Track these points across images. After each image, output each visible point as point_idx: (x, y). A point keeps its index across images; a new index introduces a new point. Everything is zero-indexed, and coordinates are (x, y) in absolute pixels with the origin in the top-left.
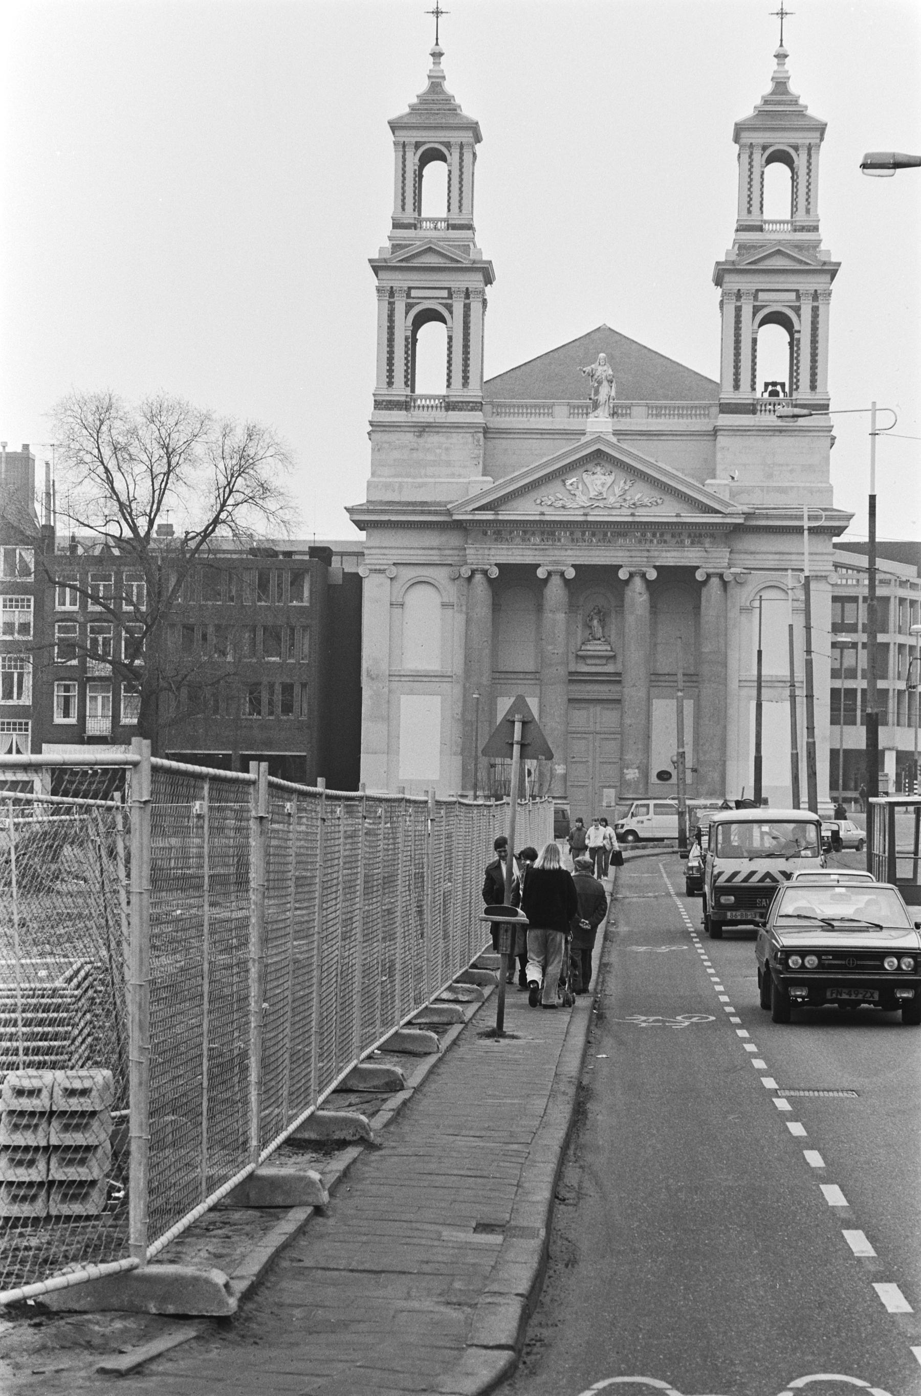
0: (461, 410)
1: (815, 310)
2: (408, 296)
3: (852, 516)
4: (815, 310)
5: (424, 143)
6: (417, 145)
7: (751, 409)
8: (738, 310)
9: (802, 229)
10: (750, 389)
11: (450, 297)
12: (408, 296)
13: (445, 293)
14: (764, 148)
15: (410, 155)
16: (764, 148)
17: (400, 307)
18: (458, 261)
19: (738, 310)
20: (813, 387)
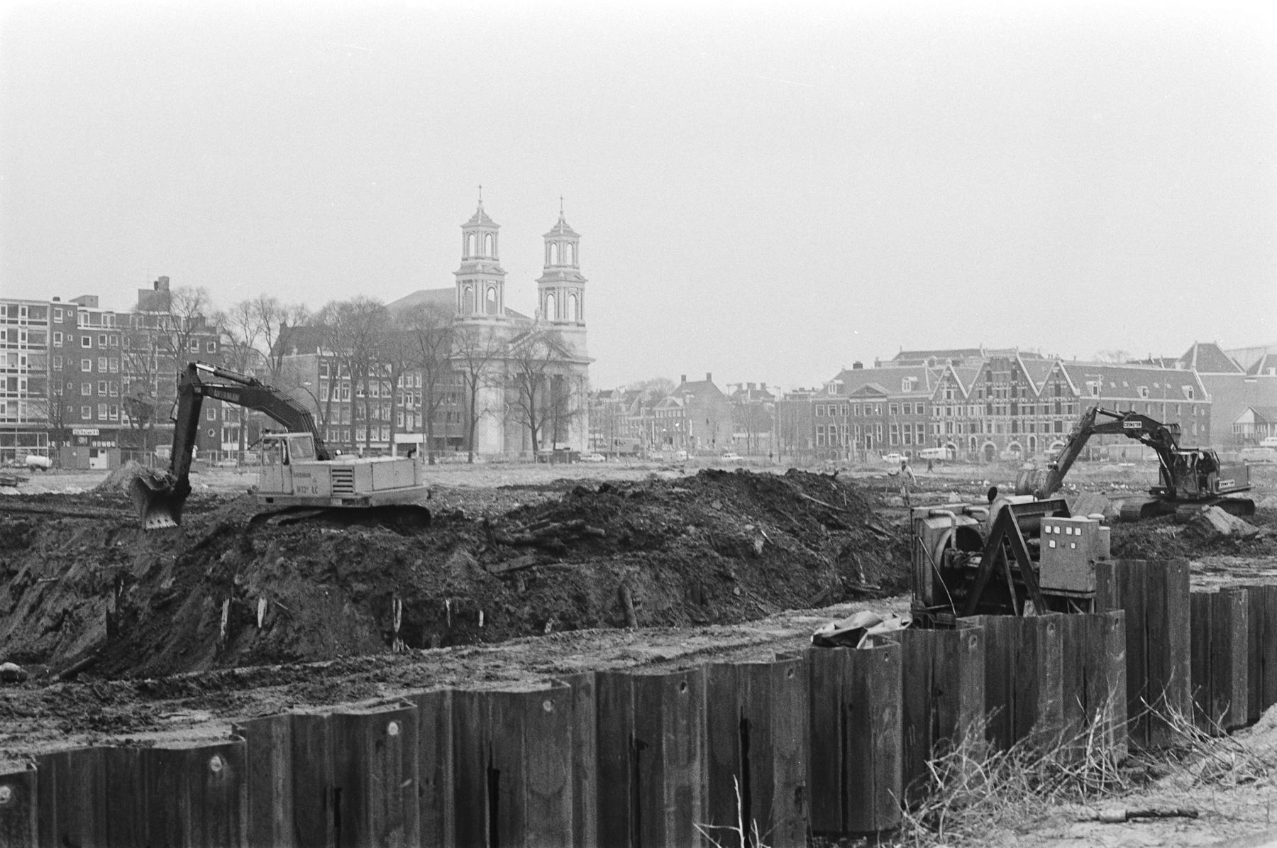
7: (567, 324)
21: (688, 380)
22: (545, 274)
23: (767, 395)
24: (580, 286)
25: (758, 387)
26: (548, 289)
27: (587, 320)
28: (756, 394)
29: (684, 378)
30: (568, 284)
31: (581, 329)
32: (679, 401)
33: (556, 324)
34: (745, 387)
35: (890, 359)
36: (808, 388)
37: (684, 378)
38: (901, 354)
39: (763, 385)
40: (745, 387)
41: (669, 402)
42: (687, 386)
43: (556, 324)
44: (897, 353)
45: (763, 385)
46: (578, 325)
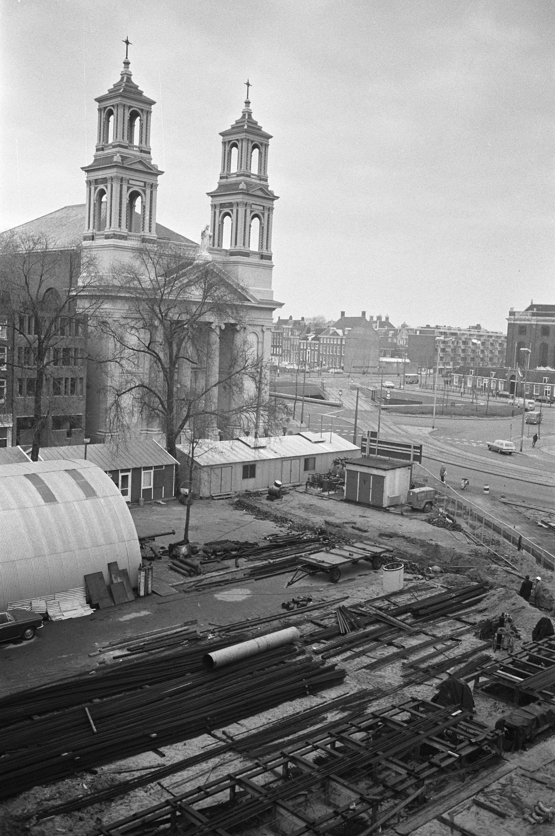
0: (150, 243)
1: (269, 215)
2: (128, 183)
3: (283, 304)
4: (269, 215)
5: (132, 107)
6: (130, 107)
7: (247, 254)
8: (246, 210)
9: (263, 180)
10: (242, 245)
11: (145, 186)
12: (128, 183)
13: (142, 184)
14: (252, 142)
15: (126, 111)
16: (252, 142)
17: (125, 188)
18: (150, 169)
19: (246, 210)
20: (267, 248)
21: (346, 316)
22: (220, 186)
23: (391, 326)
24: (266, 203)
25: (384, 319)
26: (222, 206)
27: (275, 249)
28: (382, 324)
29: (343, 313)
30: (251, 200)
31: (265, 262)
32: (340, 332)
33: (232, 254)
34: (375, 319)
35: (523, 310)
36: (433, 325)
37: (343, 313)
38: (532, 307)
39: (387, 319)
40: (375, 319)
41: (331, 332)
42: (345, 321)
43: (232, 254)
44: (529, 305)
45: (387, 319)
46: (262, 257)
